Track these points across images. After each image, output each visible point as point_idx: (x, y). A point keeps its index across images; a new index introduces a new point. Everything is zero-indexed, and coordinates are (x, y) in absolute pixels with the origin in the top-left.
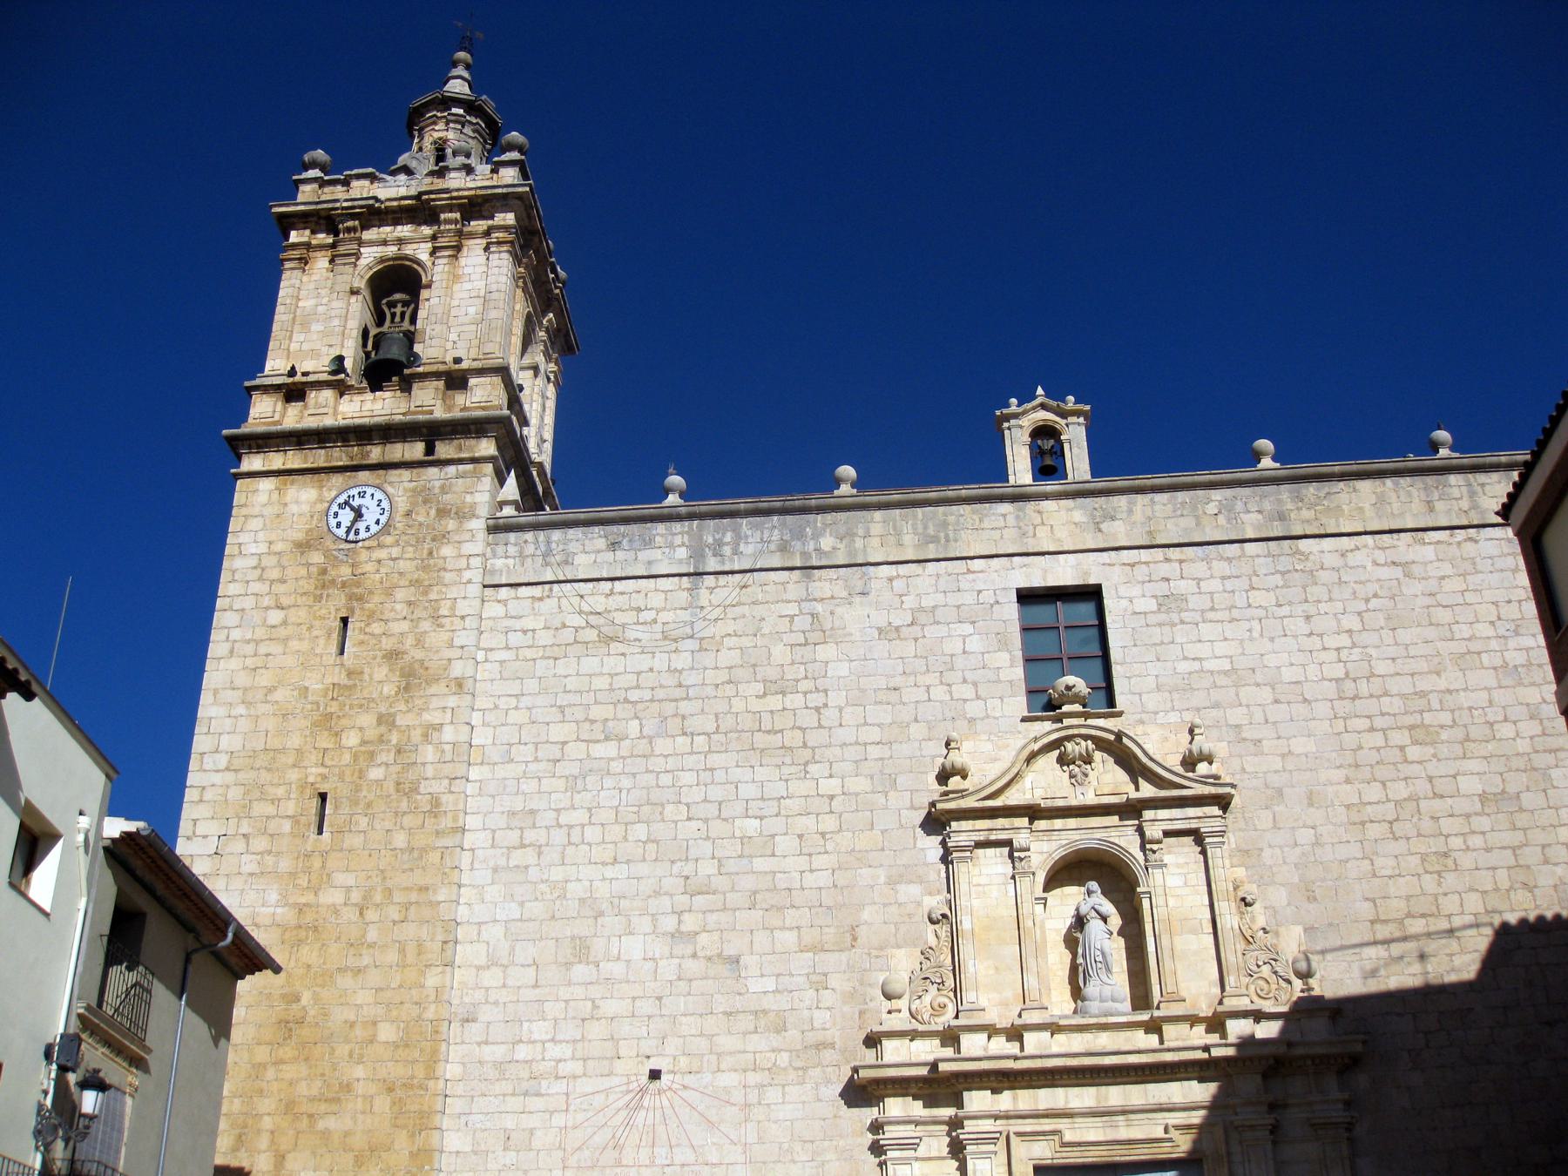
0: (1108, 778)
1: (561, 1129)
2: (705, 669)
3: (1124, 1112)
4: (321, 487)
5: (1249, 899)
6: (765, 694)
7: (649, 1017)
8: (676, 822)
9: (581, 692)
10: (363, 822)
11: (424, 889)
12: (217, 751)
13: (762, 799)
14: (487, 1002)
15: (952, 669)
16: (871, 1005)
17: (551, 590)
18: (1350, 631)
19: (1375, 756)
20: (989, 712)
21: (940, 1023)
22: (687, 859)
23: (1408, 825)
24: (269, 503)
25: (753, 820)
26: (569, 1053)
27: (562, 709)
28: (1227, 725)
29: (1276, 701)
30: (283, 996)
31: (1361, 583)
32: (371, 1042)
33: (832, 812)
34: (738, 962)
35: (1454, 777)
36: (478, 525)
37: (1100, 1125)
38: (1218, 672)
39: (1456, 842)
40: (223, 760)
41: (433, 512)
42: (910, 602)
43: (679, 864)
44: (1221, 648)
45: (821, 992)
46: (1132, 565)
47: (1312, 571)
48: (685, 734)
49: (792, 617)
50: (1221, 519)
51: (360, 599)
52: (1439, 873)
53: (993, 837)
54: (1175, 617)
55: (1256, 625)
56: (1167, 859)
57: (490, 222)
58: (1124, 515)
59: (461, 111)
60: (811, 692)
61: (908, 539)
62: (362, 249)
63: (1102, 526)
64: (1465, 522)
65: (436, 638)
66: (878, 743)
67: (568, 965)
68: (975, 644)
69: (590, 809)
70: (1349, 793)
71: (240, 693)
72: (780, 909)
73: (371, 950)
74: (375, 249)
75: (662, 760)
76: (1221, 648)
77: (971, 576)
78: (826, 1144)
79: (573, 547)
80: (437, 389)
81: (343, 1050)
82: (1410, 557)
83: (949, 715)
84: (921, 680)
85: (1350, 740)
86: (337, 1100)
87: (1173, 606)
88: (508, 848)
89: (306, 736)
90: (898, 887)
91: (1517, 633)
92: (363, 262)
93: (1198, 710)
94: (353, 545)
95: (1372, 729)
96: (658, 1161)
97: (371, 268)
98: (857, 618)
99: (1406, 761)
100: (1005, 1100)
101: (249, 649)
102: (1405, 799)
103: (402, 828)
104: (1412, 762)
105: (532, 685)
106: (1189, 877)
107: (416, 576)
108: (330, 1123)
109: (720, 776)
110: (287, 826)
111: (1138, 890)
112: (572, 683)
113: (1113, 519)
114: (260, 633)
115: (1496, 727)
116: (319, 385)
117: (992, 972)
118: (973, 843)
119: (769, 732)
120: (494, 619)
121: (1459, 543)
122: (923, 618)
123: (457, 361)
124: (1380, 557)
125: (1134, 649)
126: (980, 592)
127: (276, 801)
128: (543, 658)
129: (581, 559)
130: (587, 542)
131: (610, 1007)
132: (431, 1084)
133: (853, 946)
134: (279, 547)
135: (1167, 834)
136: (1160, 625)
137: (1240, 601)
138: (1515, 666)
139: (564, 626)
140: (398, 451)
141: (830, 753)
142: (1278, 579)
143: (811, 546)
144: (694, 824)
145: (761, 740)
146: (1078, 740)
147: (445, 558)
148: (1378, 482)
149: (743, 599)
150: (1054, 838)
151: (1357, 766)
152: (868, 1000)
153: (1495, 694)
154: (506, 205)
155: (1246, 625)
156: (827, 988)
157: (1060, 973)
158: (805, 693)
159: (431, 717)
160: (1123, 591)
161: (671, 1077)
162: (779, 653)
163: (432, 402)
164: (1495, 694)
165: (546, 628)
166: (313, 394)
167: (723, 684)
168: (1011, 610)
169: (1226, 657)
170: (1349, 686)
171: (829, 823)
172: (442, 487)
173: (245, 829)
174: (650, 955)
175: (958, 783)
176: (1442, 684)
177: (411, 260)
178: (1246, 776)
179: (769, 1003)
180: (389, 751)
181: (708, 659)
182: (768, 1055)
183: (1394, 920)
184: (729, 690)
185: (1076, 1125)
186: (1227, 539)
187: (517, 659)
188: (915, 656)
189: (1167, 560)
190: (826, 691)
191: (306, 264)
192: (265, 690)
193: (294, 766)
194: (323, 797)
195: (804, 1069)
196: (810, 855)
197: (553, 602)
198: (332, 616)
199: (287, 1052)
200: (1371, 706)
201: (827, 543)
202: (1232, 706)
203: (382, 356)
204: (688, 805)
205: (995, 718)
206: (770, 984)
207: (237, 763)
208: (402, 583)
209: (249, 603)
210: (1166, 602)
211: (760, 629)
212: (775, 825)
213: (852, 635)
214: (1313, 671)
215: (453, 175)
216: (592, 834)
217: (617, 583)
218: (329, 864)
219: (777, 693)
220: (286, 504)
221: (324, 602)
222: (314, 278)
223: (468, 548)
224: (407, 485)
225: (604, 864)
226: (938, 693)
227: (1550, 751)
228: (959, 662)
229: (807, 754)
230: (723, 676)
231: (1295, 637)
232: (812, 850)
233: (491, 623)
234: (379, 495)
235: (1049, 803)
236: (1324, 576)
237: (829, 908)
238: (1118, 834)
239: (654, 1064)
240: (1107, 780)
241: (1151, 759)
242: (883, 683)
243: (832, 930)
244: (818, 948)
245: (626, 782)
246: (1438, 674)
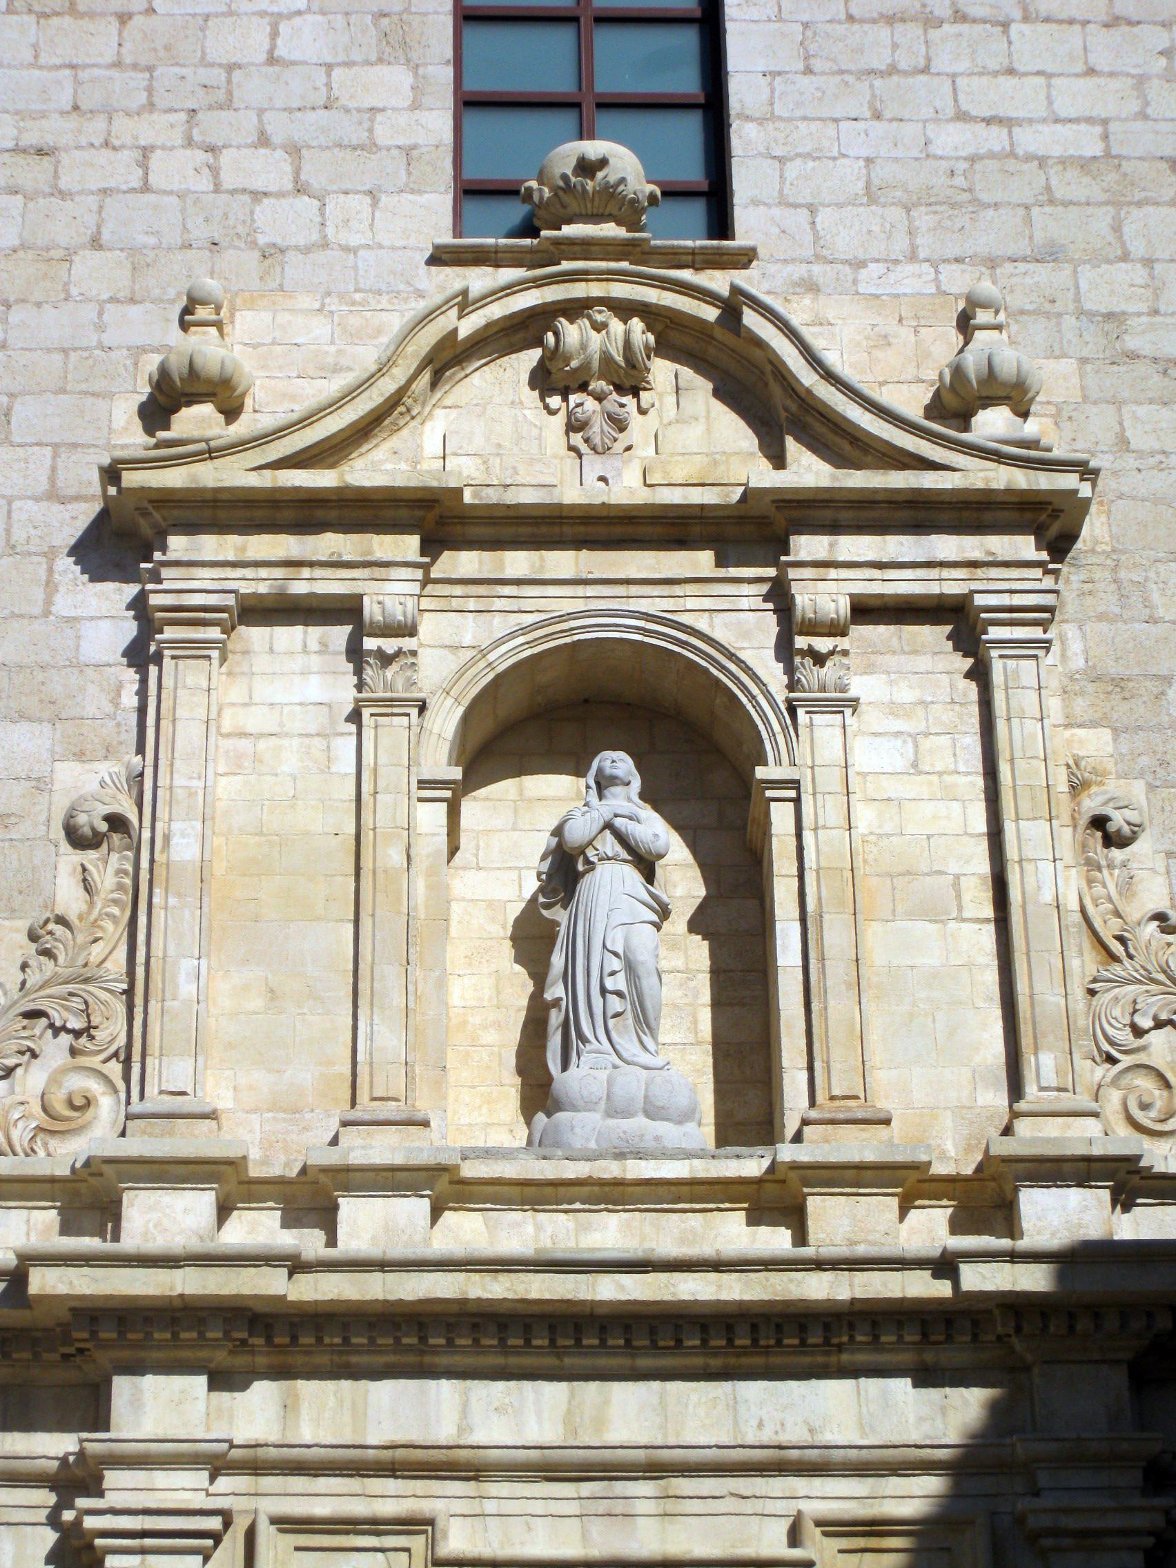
0: (690, 437)
3: (655, 1469)
5: (1118, 821)
15: (227, 104)
20: (330, 231)
28: (1081, 313)
37: (573, 1508)
38: (1063, 162)
53: (299, 588)
83: (200, 232)
84: (124, 129)
93: (992, 263)
106: (925, 744)
111: (760, 772)
117: (256, 1002)
118: (230, 600)
125: (806, 81)
150: (499, 604)
157: (490, 1037)
169: (1090, 120)
175: (203, 420)
178: (1131, 462)
185: (490, 1507)
188: (118, 64)
202: (1097, 259)
205: (347, 249)
228: (252, 88)
238: (707, 603)
241: (829, 376)
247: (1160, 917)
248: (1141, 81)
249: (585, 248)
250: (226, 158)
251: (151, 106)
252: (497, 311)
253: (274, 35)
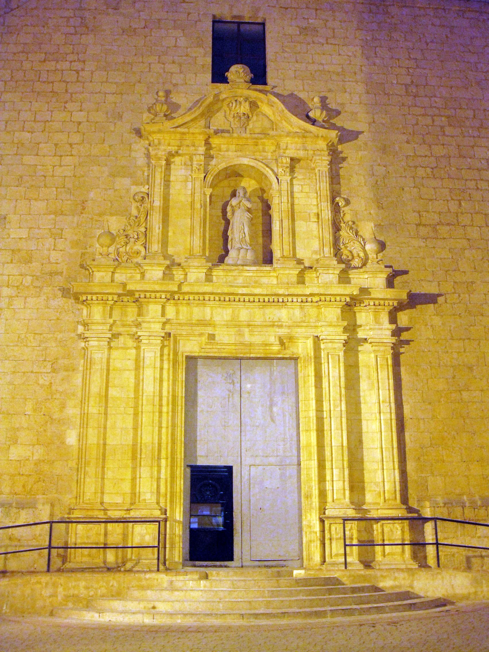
6: (45, 61)
13: (35, 121)
16: (89, 250)
25: (27, 133)
33: (78, 132)
34: (5, 218)
45: (57, 240)
60: (75, 61)
66: (114, 94)
68: (182, 42)
78: (49, 336)
99: (444, 134)
102: (442, 156)
104: (448, 136)
106: (304, 187)
124: (437, 22)
133: (82, 213)
145: (38, 86)
152: (88, 247)
156: (61, 238)
157: (217, 242)
158: (71, 62)
167: (19, 53)
171: (76, 138)
182: (18, 277)
184: (23, 57)
190: (84, 62)
196: (61, 156)
206: (24, 233)
230: (20, 48)
243: (69, 202)
253: (176, 41)
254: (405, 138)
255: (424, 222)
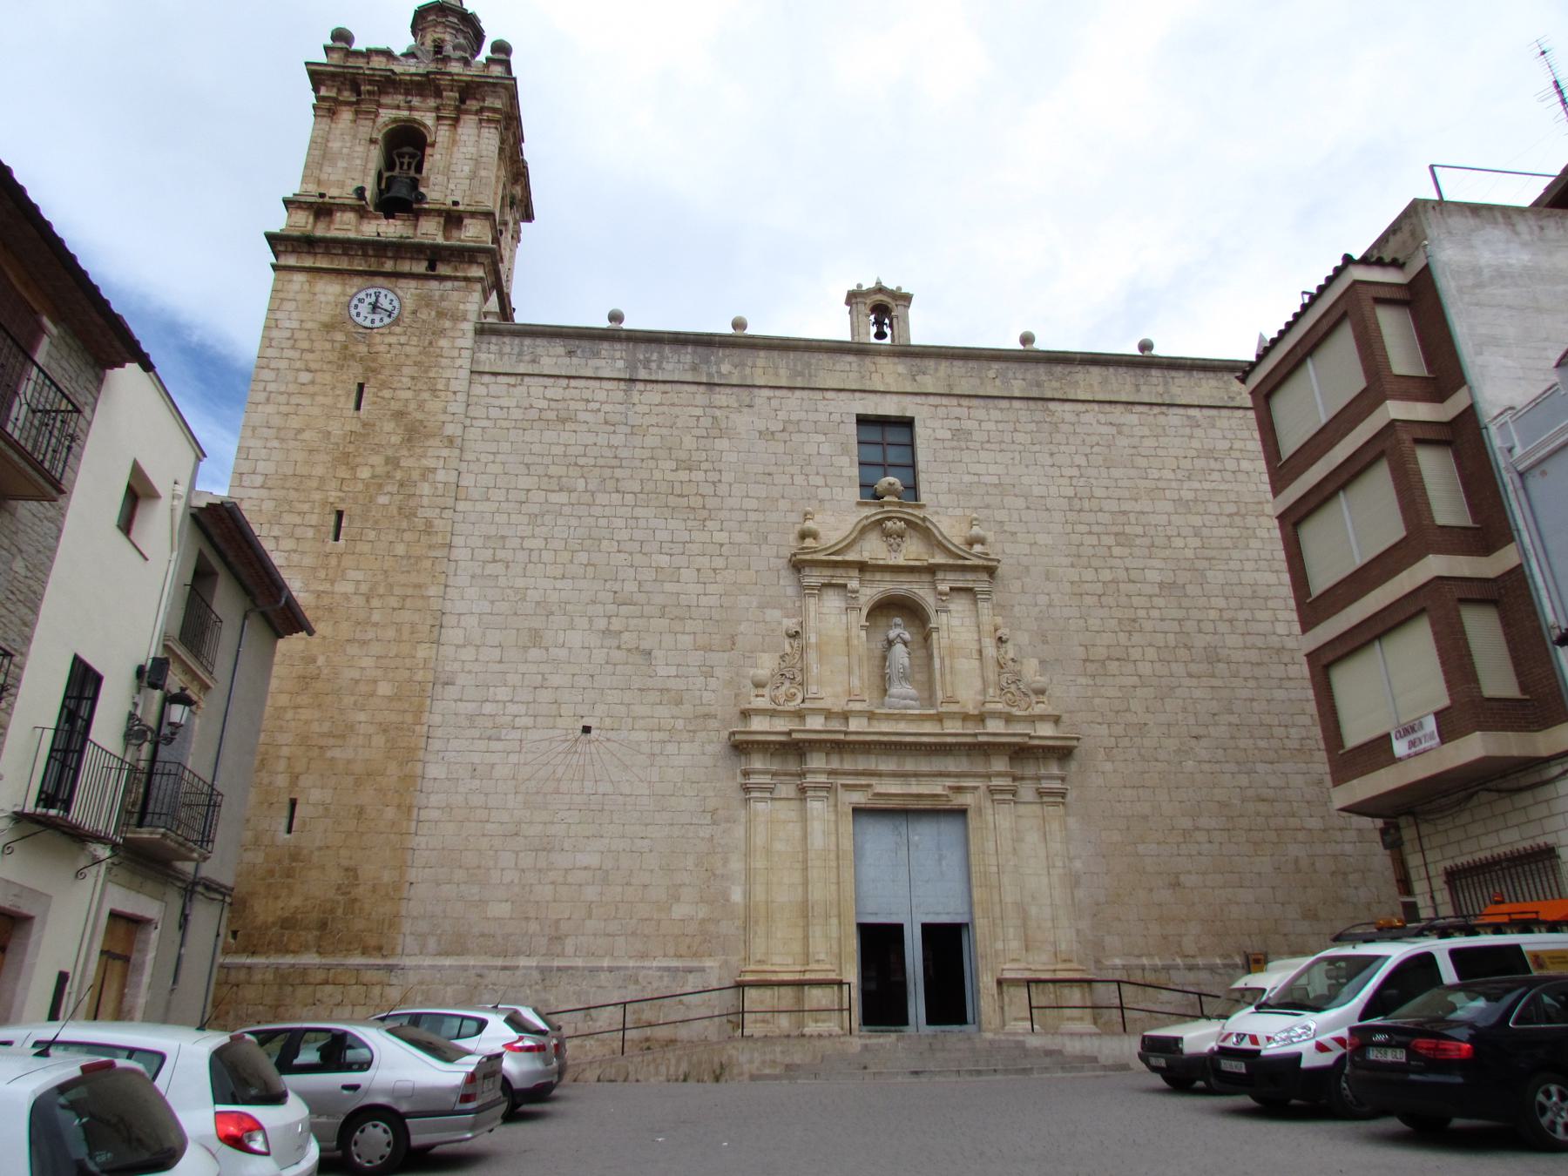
1: (515, 764)
2: (635, 447)
4: (344, 284)
5: (1004, 638)
6: (677, 470)
7: (584, 688)
8: (609, 553)
9: (543, 455)
10: (372, 535)
11: (418, 586)
12: (254, 473)
13: (672, 542)
14: (463, 671)
15: (809, 464)
17: (522, 380)
18: (1079, 466)
19: (1090, 551)
21: (792, 706)
22: (616, 580)
23: (1111, 599)
24: (301, 291)
26: (523, 712)
27: (528, 466)
29: (1028, 508)
30: (303, 658)
31: (1089, 435)
32: (372, 695)
35: (1143, 569)
36: (468, 327)
38: (991, 485)
39: (1142, 613)
40: (259, 480)
41: (433, 313)
42: (782, 415)
43: (610, 582)
44: (992, 469)
46: (936, 406)
47: (1056, 423)
48: (618, 491)
49: (699, 417)
50: (998, 382)
51: (373, 370)
52: (1130, 632)
53: (834, 582)
54: (963, 445)
55: (1017, 455)
56: (952, 607)
57: (481, 104)
58: (932, 372)
59: (456, 21)
61: (783, 372)
62: (380, 111)
63: (917, 378)
64: (1160, 401)
65: (434, 405)
67: (526, 648)
68: (825, 449)
69: (546, 539)
70: (1073, 574)
71: (275, 430)
72: (682, 619)
73: (375, 629)
74: (390, 111)
75: (600, 508)
76: (992, 469)
77: (825, 402)
78: (708, 784)
79: (539, 351)
80: (439, 223)
81: (348, 700)
82: (1122, 420)
83: (805, 496)
85: (1075, 538)
86: (343, 737)
87: (962, 436)
88: (483, 562)
89: (327, 468)
90: (765, 610)
91: (1189, 478)
92: (380, 120)
94: (369, 331)
95: (1090, 533)
96: (586, 791)
97: (386, 125)
98: (743, 422)
99: (1111, 556)
100: (835, 764)
101: (283, 399)
103: (402, 541)
105: (505, 447)
107: (419, 359)
108: (336, 753)
109: (642, 523)
110: (310, 533)
112: (536, 448)
113: (924, 374)
114: (292, 388)
115: (1172, 539)
116: (344, 208)
119: (679, 496)
120: (478, 396)
121: (1155, 415)
122: (791, 428)
123: (455, 203)
124: (1103, 419)
126: (830, 414)
127: (302, 514)
128: (514, 428)
129: (545, 360)
130: (550, 349)
131: (555, 680)
132: (418, 728)
134: (309, 325)
135: (951, 589)
136: (953, 449)
137: (1007, 438)
138: (1187, 501)
139: (531, 407)
140: (405, 267)
141: (723, 514)
142: (1033, 427)
143: (714, 369)
144: (623, 556)
145: (672, 501)
146: (895, 520)
147: (442, 348)
148: (1104, 368)
149: (664, 402)
151: (1079, 556)
153: (1173, 518)
154: (495, 92)
155: (1010, 455)
158: (706, 471)
159: (429, 463)
160: (929, 423)
161: (598, 731)
162: (689, 442)
163: (435, 232)
164: (1173, 518)
165: (517, 407)
166: (338, 214)
168: (852, 428)
170: (1077, 504)
172: (442, 296)
173: (276, 532)
174: (587, 645)
176: (1138, 508)
177: (419, 124)
179: (672, 684)
180: (394, 484)
181: (637, 441)
183: (1098, 661)
184: (652, 464)
186: (1000, 395)
187: (495, 427)
189: (959, 405)
190: (720, 471)
191: (334, 113)
192: (294, 432)
193: (317, 489)
194: (340, 514)
195: (694, 732)
197: (523, 389)
198: (351, 381)
199: (304, 699)
200: (1091, 518)
201: (725, 368)
203: (392, 194)
204: (618, 541)
205: (838, 501)
206: (673, 671)
207: (270, 484)
208: (408, 363)
209: (283, 364)
210: (957, 433)
211: (675, 423)
212: (680, 561)
213: (739, 434)
214: (1053, 490)
215: (453, 64)
216: (547, 556)
217: (572, 381)
218: (343, 564)
219: (685, 469)
220: (315, 294)
221: (345, 370)
222: (340, 126)
223: (460, 343)
224: (413, 290)
225: (555, 578)
226: (799, 480)
227: (1207, 559)
229: (705, 513)
230: (647, 454)
231: (1043, 466)
232: (706, 580)
233: (475, 399)
234: (391, 296)
235: (874, 562)
236: (1064, 428)
237: (717, 621)
239: (587, 722)
240: (912, 551)
241: (945, 538)
242: (760, 469)
243: (718, 636)
244: (708, 649)
245: (574, 522)
246: (1136, 500)
247: (1012, 659)
248: (1007, 465)
249: (890, 503)
250: (810, 477)
251: (793, 464)
252: (873, 519)
254: (1066, 561)
255: (1091, 658)
